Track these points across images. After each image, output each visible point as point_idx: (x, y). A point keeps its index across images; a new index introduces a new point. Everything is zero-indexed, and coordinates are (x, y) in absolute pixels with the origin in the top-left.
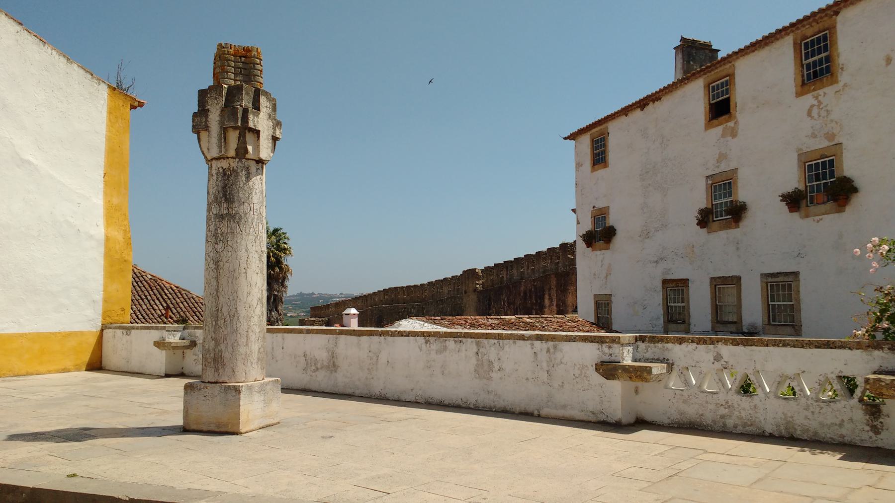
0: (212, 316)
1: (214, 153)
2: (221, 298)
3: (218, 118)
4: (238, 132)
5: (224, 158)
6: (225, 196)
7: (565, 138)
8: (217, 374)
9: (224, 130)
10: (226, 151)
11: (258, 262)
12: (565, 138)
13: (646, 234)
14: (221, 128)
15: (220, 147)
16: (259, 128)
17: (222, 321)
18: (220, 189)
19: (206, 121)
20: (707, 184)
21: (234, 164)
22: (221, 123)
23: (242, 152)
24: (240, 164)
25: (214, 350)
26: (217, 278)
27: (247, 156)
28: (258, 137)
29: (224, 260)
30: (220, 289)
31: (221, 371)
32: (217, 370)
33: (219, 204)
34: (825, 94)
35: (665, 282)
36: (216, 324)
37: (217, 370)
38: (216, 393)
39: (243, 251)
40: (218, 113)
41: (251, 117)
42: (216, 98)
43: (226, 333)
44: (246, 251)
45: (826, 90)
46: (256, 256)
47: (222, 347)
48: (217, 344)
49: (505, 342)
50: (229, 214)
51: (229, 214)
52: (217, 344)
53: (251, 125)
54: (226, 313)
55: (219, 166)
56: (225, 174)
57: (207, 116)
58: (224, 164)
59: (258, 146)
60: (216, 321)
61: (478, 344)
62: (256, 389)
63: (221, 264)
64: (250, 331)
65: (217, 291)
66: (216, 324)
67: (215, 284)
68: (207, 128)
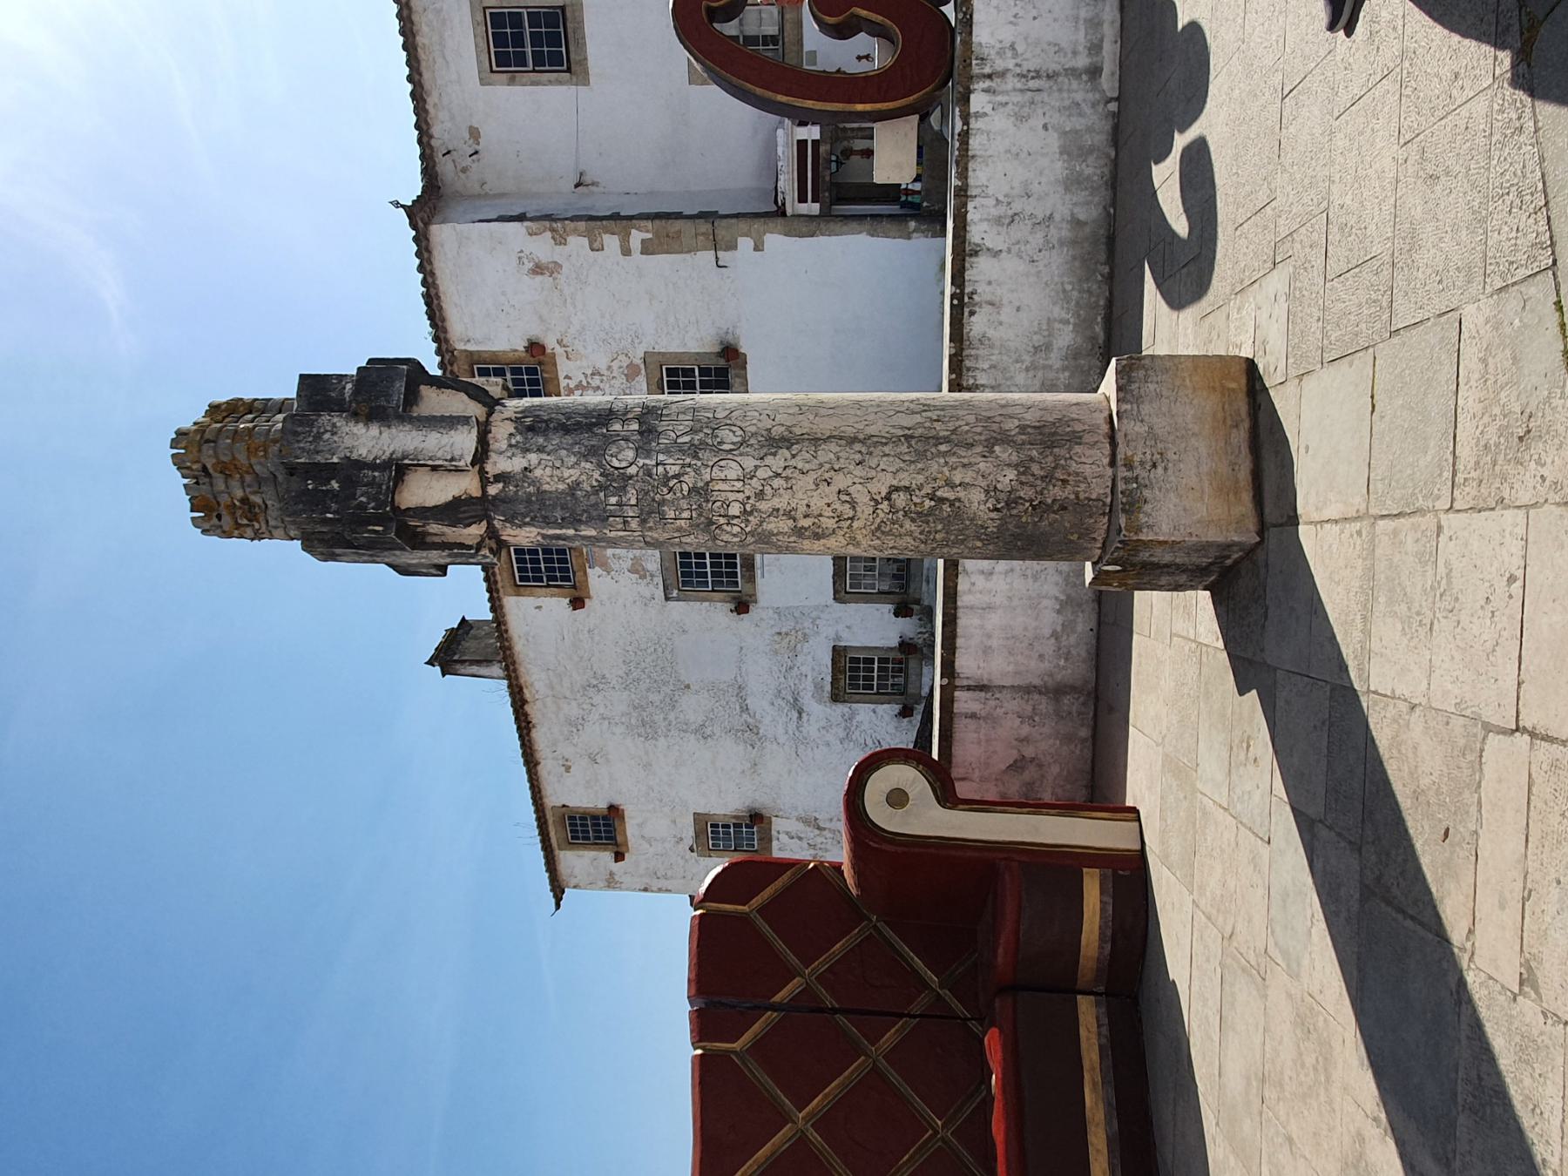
0: (921, 455)
2: (871, 430)
6: (589, 427)
7: (558, 906)
8: (1087, 438)
12: (558, 906)
13: (751, 732)
17: (937, 425)
18: (569, 439)
19: (373, 466)
20: (678, 599)
25: (1019, 447)
26: (816, 441)
29: (768, 424)
30: (850, 431)
31: (1078, 427)
32: (1076, 438)
33: (610, 440)
34: (567, 377)
35: (836, 698)
36: (947, 440)
37: (1076, 438)
38: (1141, 429)
40: (359, 429)
43: (971, 419)
45: (561, 376)
47: (1011, 425)
48: (1005, 439)
49: (971, 181)
50: (640, 419)
51: (640, 419)
52: (1005, 439)
54: (918, 418)
56: (531, 429)
57: (360, 465)
60: (938, 440)
61: (975, 253)
63: (778, 431)
65: (853, 440)
66: (947, 440)
67: (833, 447)
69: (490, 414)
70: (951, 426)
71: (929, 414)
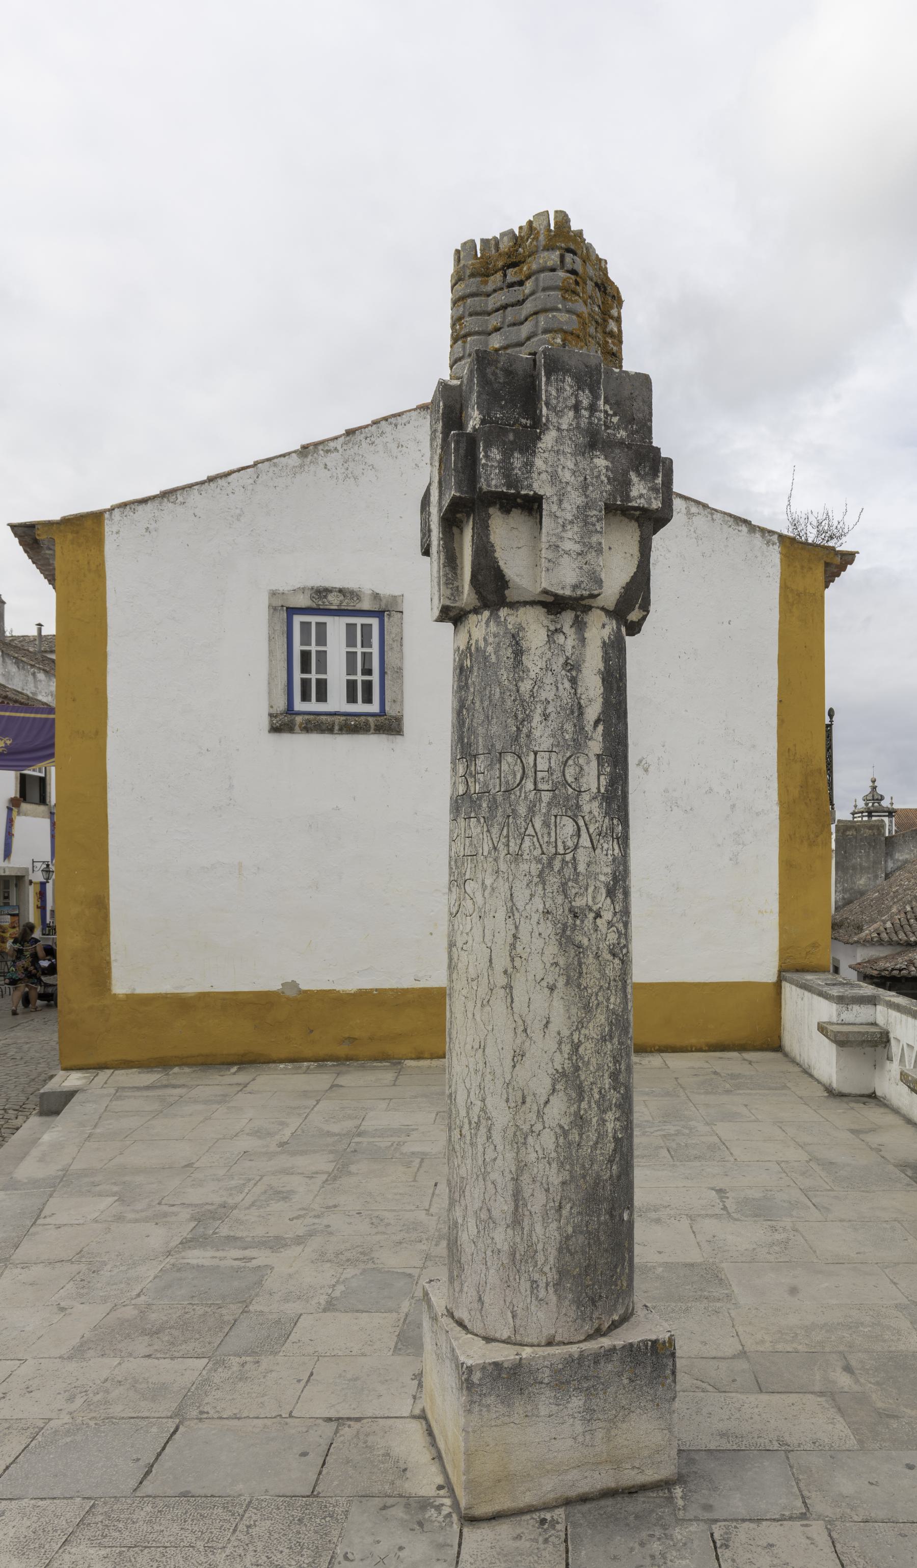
11: (552, 949)
27: (511, 595)
39: (501, 914)
44: (512, 911)
46: (547, 928)
62: (545, 1375)
64: (525, 1178)
69: (476, 611)
70: (457, 1147)
71: (466, 1126)
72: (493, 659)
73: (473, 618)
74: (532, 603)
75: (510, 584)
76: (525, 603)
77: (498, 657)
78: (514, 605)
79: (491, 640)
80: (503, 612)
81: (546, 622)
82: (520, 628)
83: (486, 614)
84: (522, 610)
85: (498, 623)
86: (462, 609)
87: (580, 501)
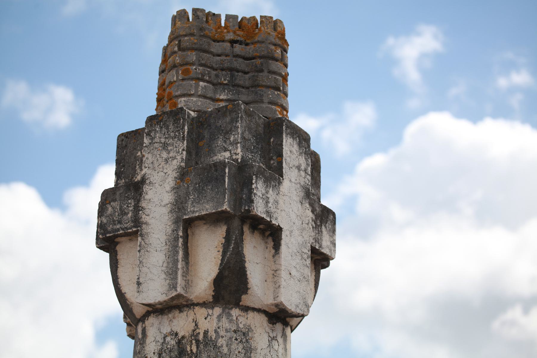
1: (155, 292)
3: (168, 198)
4: (221, 232)
5: (180, 308)
9: (186, 227)
10: (188, 285)
14: (176, 222)
15: (172, 273)
16: (280, 219)
19: (137, 208)
21: (209, 321)
22: (178, 206)
23: (230, 286)
24: (225, 323)
27: (246, 300)
28: (277, 247)
40: (170, 183)
41: (259, 187)
42: (165, 146)
53: (259, 209)
55: (166, 329)
58: (182, 324)
59: (275, 273)
68: (136, 231)
72: (225, 350)
73: (201, 312)
74: (259, 311)
75: (249, 292)
76: (254, 309)
77: (229, 350)
78: (246, 309)
79: (222, 333)
80: (235, 312)
81: (268, 329)
82: (250, 329)
83: (217, 311)
84: (251, 314)
85: (231, 321)
86: (188, 300)
87: (300, 239)
